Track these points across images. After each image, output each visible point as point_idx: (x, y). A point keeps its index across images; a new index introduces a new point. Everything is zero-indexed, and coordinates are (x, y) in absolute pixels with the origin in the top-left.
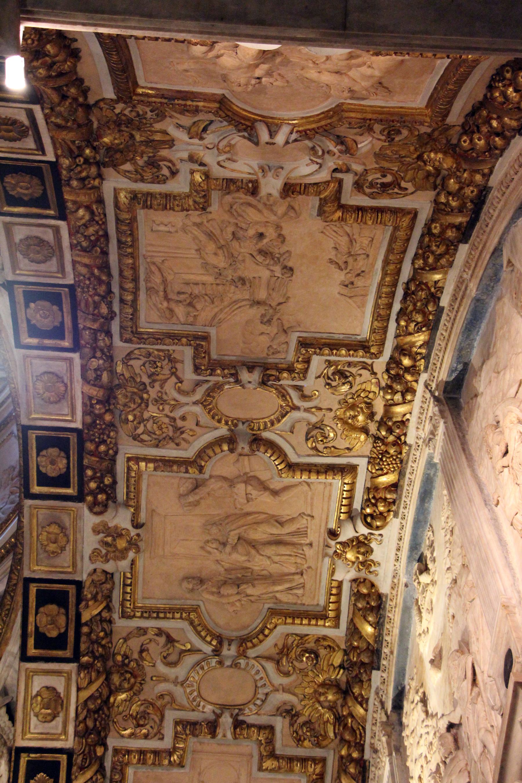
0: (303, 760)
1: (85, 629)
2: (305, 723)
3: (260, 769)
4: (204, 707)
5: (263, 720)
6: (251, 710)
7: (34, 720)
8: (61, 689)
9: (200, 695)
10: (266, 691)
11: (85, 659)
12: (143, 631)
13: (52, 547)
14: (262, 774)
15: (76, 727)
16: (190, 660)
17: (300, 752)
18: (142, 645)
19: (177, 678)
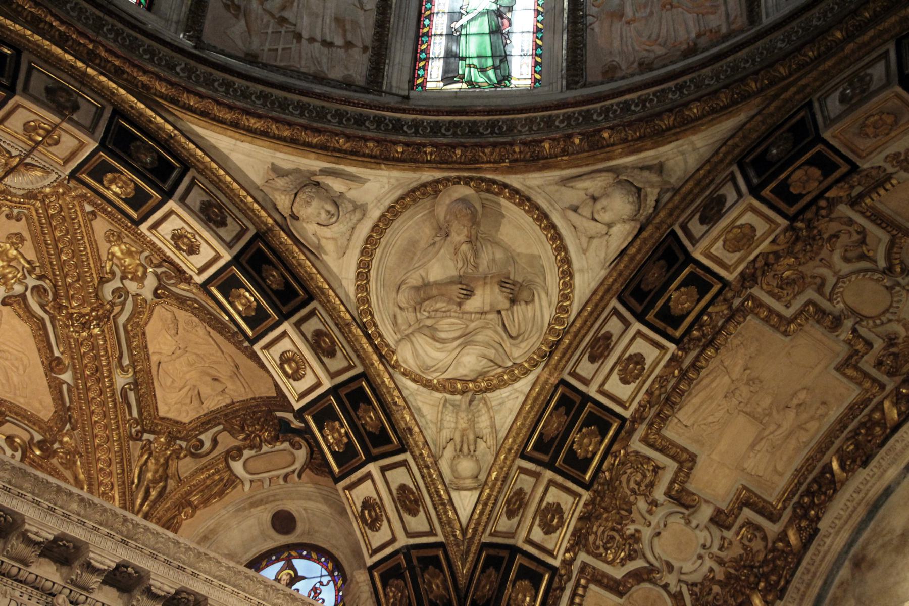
0: (874, 380)
1: (823, 203)
2: (893, 354)
3: (837, 369)
4: (838, 302)
5: (870, 336)
6: (868, 324)
7: (720, 243)
8: (759, 233)
9: (842, 293)
10: (891, 317)
11: (800, 224)
12: (851, 222)
13: (870, 131)
14: (835, 373)
15: (747, 267)
16: (864, 264)
17: (874, 372)
18: (840, 231)
19: (840, 270)
